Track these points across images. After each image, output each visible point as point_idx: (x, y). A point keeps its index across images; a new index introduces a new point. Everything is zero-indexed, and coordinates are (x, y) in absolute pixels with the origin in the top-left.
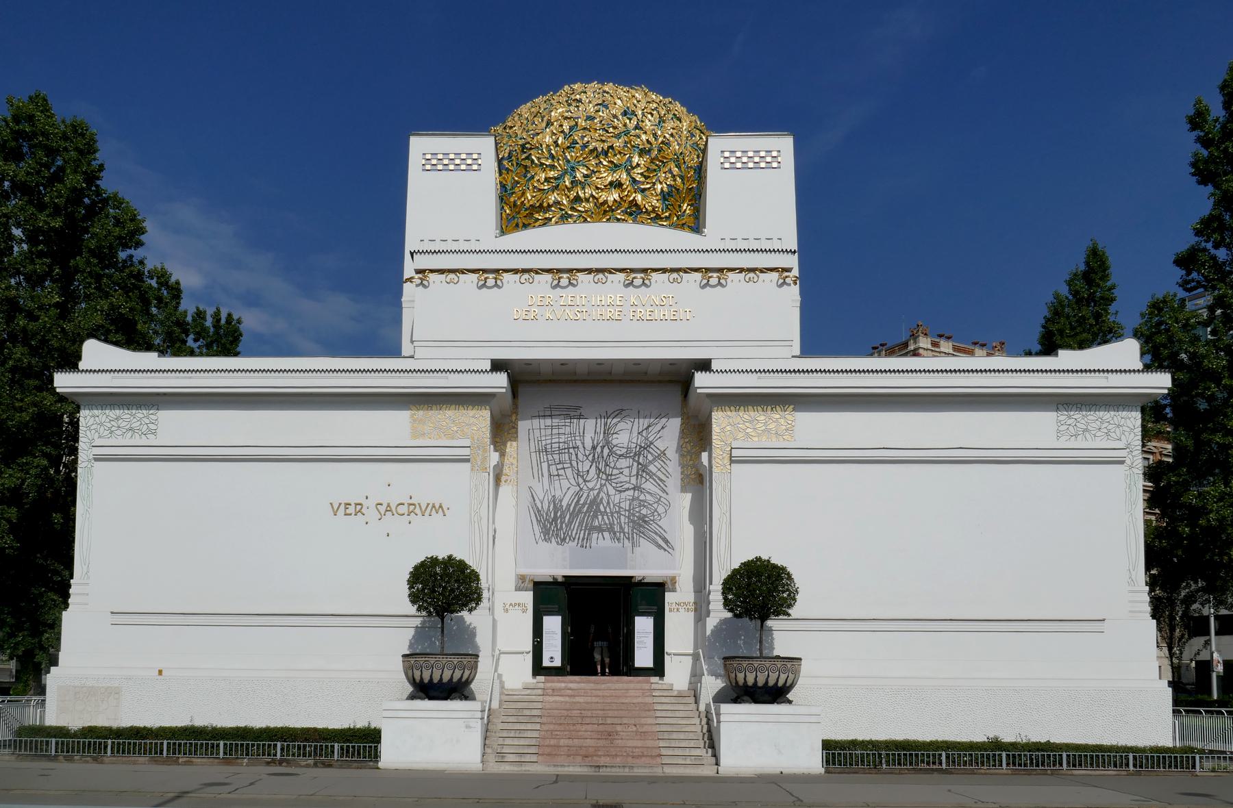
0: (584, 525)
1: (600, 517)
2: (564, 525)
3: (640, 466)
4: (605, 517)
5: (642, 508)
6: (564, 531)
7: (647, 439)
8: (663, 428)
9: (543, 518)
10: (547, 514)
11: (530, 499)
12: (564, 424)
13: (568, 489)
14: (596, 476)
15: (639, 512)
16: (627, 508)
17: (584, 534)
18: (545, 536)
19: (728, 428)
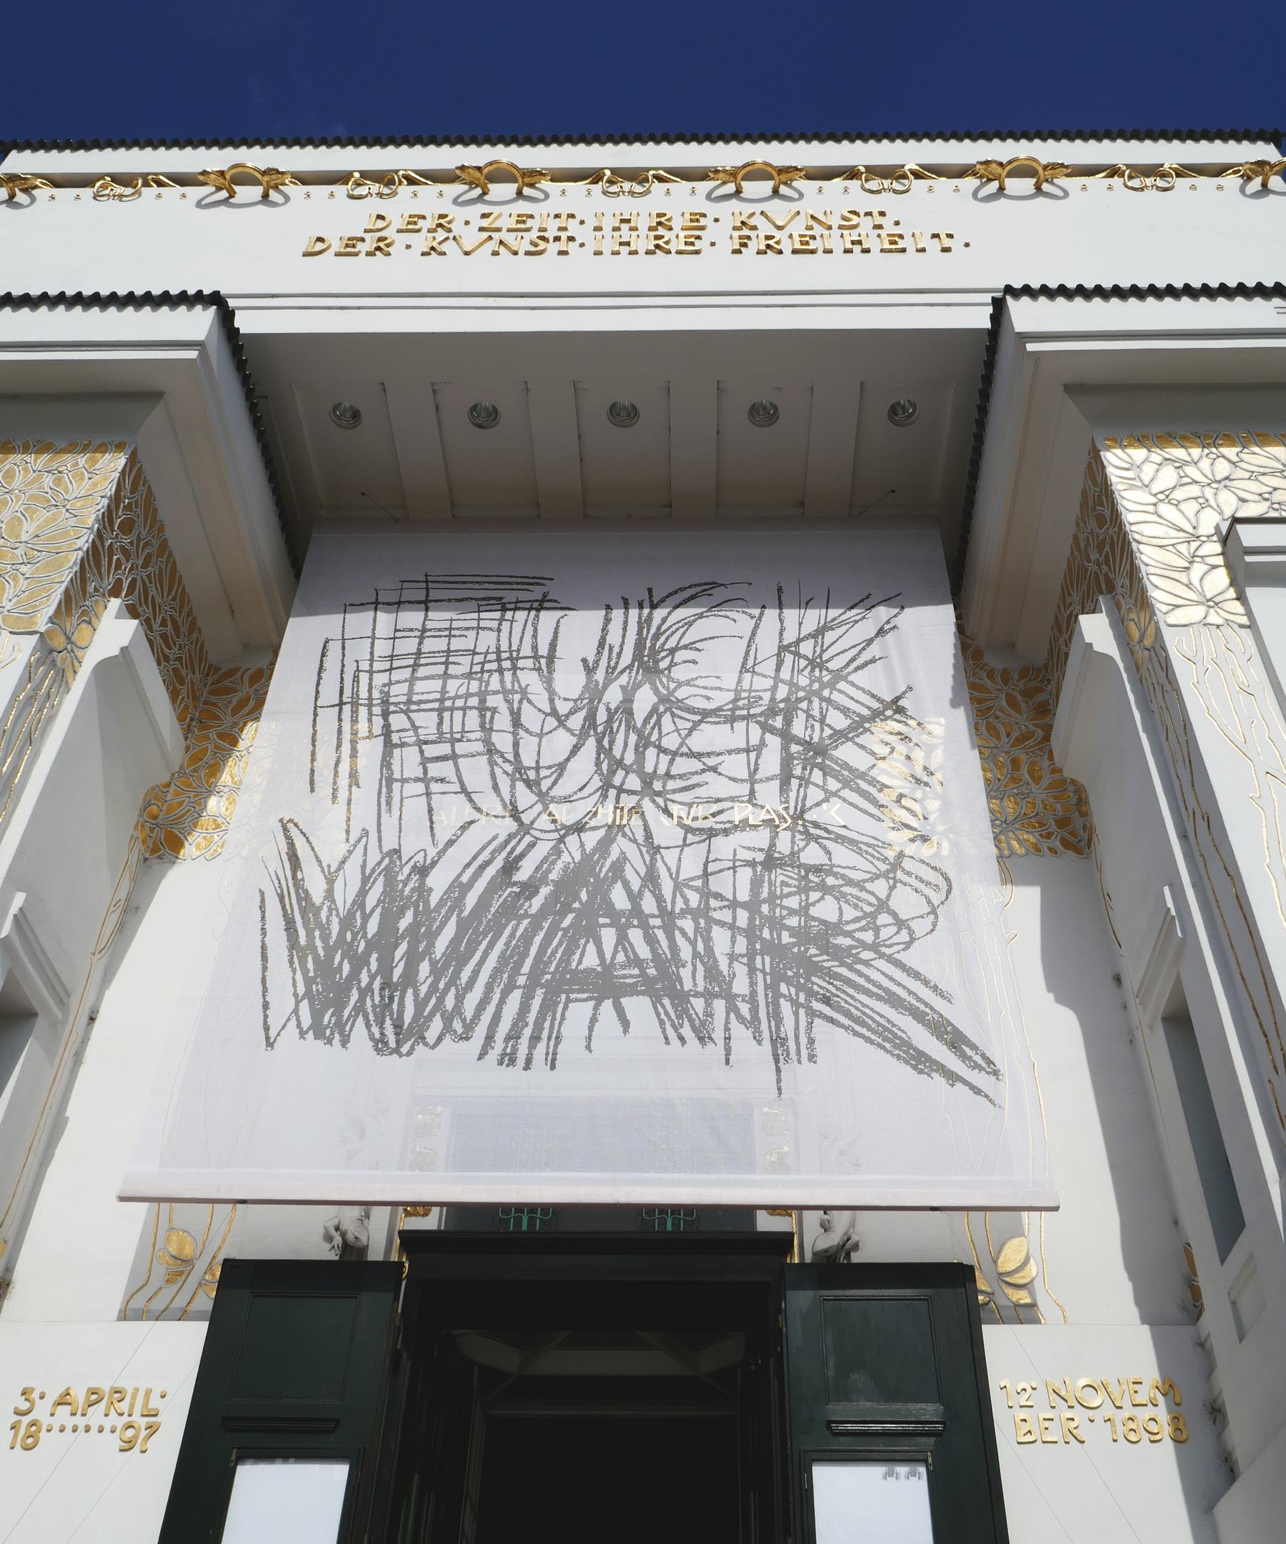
0: (526, 968)
1: (609, 937)
2: (424, 968)
3: (795, 748)
4: (635, 935)
5: (814, 896)
6: (423, 989)
7: (816, 663)
8: (881, 632)
9: (325, 938)
10: (346, 923)
11: (284, 869)
12: (474, 624)
13: (464, 828)
14: (597, 782)
15: (804, 911)
16: (743, 896)
17: (524, 1008)
18: (317, 1015)
19: (1194, 490)
